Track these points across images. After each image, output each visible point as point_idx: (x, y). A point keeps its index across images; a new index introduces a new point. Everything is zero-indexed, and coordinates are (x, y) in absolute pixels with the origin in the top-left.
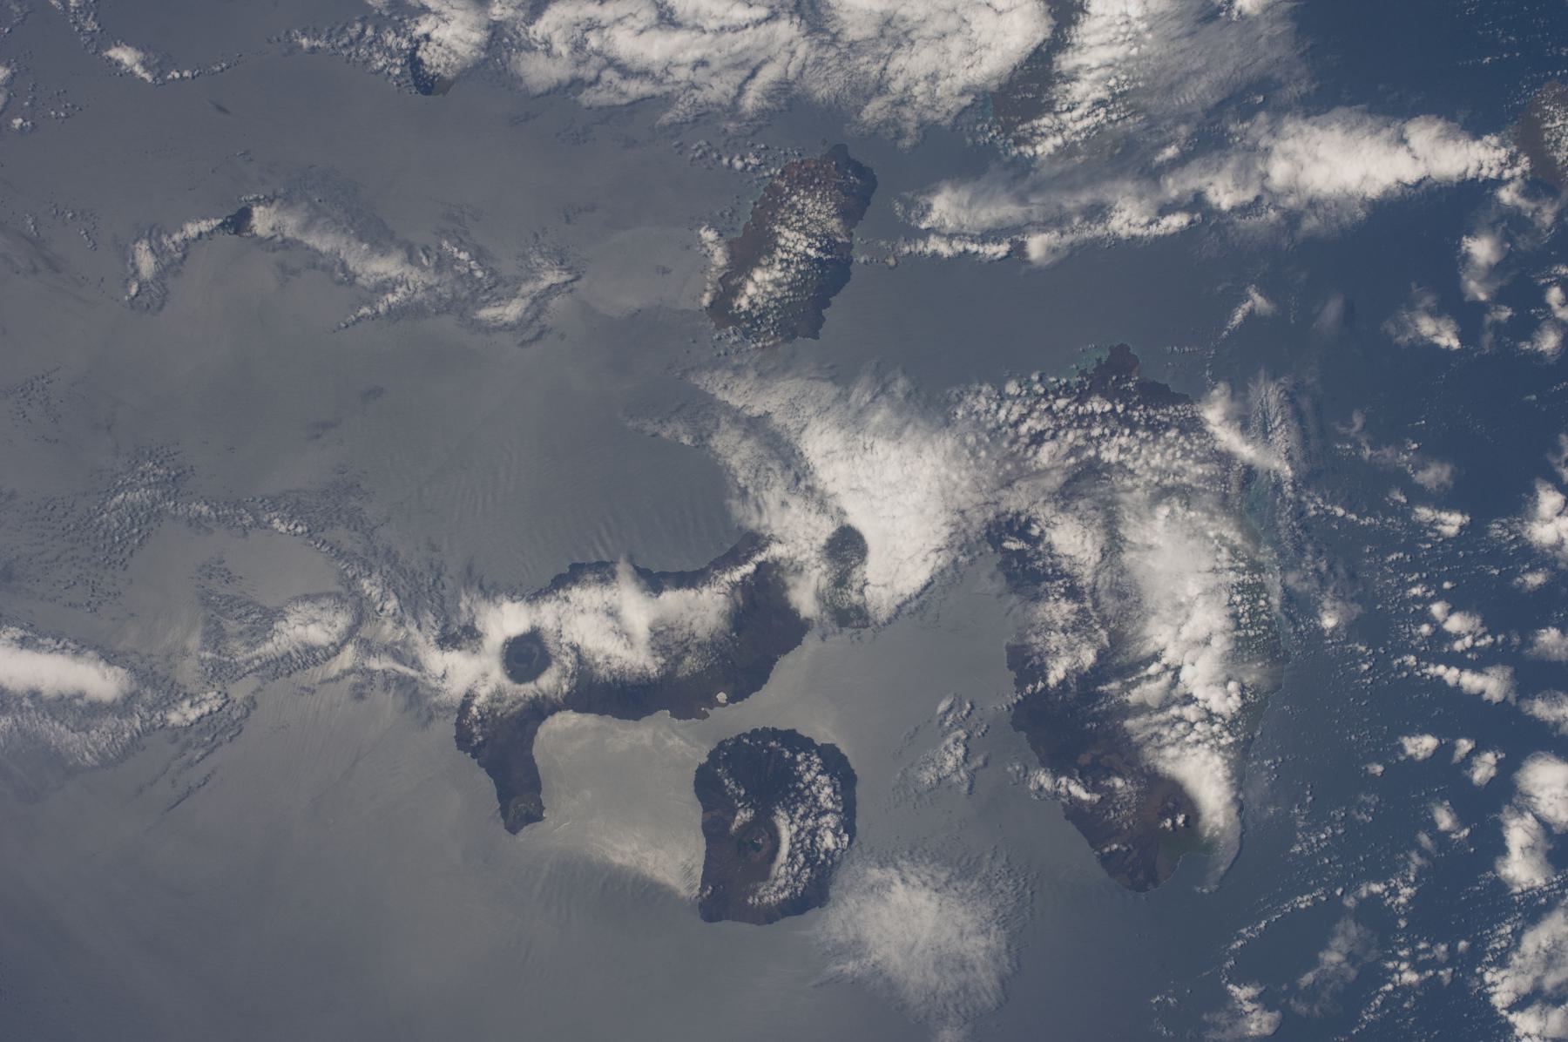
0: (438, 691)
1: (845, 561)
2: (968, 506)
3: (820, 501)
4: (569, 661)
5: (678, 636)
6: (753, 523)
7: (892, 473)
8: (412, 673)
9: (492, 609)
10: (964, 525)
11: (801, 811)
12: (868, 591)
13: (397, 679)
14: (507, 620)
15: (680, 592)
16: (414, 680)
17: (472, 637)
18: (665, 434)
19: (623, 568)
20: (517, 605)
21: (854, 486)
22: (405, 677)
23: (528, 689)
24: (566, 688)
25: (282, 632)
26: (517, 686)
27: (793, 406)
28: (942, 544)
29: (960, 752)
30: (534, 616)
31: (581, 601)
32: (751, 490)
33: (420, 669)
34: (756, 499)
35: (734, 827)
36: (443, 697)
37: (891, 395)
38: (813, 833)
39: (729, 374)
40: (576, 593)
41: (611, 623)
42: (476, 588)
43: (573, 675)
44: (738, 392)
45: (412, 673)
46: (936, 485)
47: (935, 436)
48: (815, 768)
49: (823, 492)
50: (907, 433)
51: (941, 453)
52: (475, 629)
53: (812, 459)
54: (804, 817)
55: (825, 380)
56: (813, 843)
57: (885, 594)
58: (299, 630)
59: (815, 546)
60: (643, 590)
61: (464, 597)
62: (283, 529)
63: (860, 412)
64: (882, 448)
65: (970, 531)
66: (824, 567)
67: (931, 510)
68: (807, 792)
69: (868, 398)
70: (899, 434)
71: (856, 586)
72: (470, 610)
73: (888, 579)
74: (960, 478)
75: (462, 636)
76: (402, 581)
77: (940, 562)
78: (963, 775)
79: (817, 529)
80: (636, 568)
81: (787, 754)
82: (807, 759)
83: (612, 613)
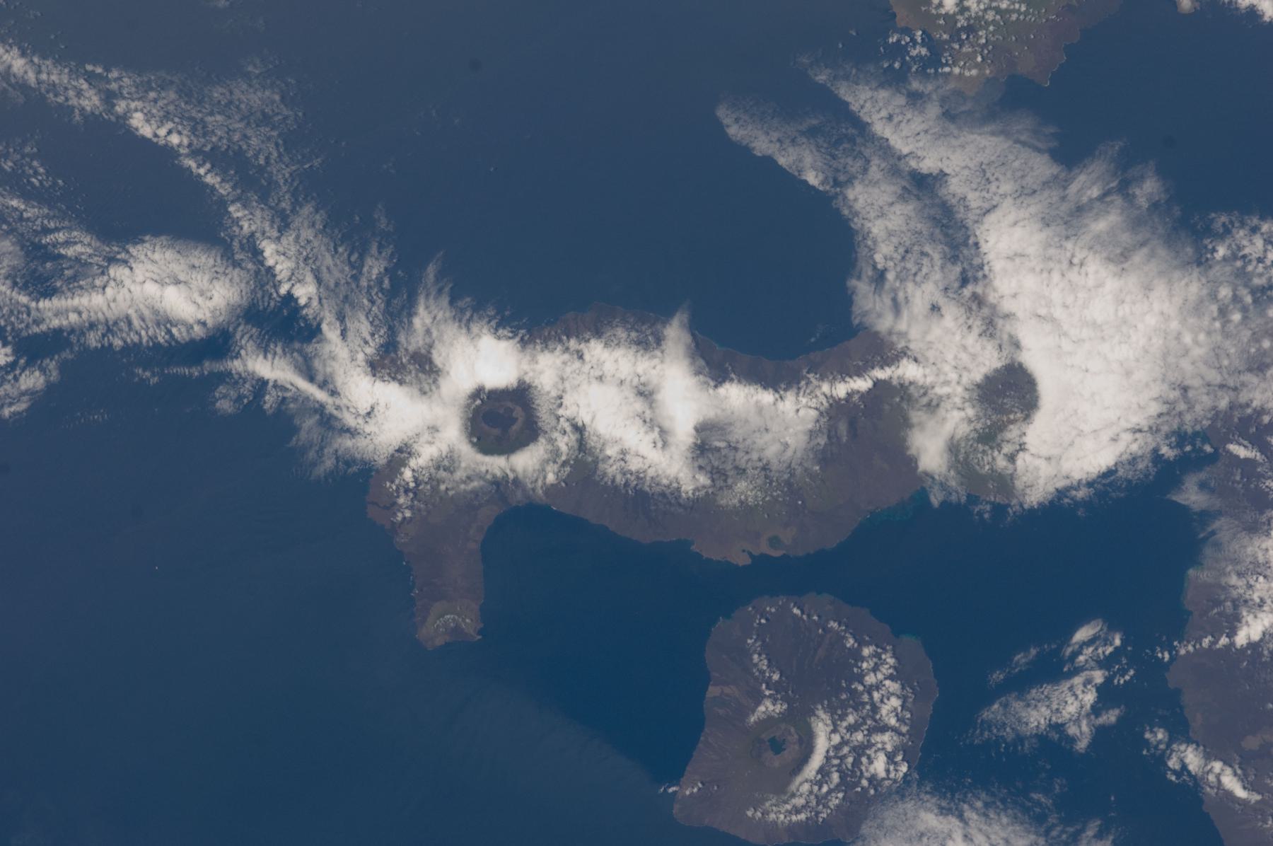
0: (352, 432)
1: (1001, 410)
2: (1196, 382)
3: (990, 320)
4: (565, 443)
5: (741, 459)
6: (884, 323)
7: (1101, 309)
8: (321, 395)
9: (463, 339)
10: (1182, 406)
11: (851, 719)
12: (1023, 460)
13: (295, 399)
14: (484, 360)
15: (751, 390)
16: (320, 409)
17: (424, 371)
18: (782, 161)
19: (675, 333)
20: (504, 345)
21: (1043, 312)
22: (307, 398)
23: (496, 464)
24: (551, 478)
25: (120, 284)
26: (480, 457)
27: (984, 176)
28: (1144, 424)
29: (1090, 698)
30: (525, 367)
31: (600, 364)
32: (890, 276)
33: (334, 393)
34: (895, 291)
35: (753, 719)
36: (362, 443)
37: (1129, 198)
38: (860, 751)
39: (901, 100)
40: (595, 349)
41: (641, 407)
42: (445, 301)
43: (565, 464)
44: (906, 130)
45: (321, 395)
46: (1158, 342)
47: (1177, 274)
48: (885, 670)
49: (994, 307)
50: (1138, 257)
51: (1178, 300)
52: (431, 362)
53: (990, 257)
54: (852, 729)
55: (1039, 150)
56: (857, 763)
57: (1045, 470)
58: (151, 289)
59: (965, 380)
60: (698, 373)
61: (421, 309)
62: (147, 131)
63: (1079, 210)
64: (1096, 269)
65: (1188, 418)
66: (970, 412)
67: (1141, 375)
68: (866, 698)
69: (1095, 192)
70: (1125, 256)
71: (1007, 449)
72: (428, 332)
73: (1055, 452)
74: (1196, 342)
75: (400, 362)
76: (329, 260)
77: (1134, 447)
78: (1085, 728)
79: (974, 357)
80: (693, 335)
81: (850, 642)
82: (878, 655)
83: (646, 393)
